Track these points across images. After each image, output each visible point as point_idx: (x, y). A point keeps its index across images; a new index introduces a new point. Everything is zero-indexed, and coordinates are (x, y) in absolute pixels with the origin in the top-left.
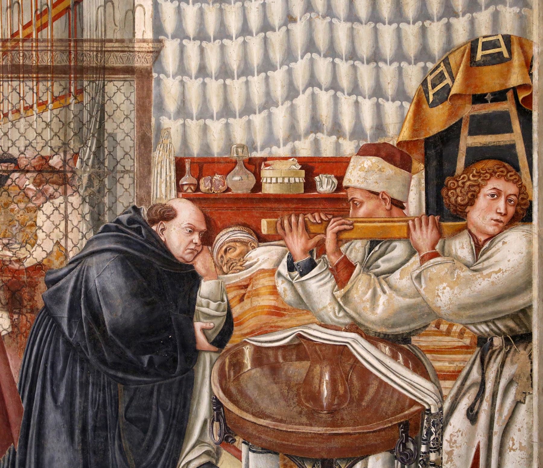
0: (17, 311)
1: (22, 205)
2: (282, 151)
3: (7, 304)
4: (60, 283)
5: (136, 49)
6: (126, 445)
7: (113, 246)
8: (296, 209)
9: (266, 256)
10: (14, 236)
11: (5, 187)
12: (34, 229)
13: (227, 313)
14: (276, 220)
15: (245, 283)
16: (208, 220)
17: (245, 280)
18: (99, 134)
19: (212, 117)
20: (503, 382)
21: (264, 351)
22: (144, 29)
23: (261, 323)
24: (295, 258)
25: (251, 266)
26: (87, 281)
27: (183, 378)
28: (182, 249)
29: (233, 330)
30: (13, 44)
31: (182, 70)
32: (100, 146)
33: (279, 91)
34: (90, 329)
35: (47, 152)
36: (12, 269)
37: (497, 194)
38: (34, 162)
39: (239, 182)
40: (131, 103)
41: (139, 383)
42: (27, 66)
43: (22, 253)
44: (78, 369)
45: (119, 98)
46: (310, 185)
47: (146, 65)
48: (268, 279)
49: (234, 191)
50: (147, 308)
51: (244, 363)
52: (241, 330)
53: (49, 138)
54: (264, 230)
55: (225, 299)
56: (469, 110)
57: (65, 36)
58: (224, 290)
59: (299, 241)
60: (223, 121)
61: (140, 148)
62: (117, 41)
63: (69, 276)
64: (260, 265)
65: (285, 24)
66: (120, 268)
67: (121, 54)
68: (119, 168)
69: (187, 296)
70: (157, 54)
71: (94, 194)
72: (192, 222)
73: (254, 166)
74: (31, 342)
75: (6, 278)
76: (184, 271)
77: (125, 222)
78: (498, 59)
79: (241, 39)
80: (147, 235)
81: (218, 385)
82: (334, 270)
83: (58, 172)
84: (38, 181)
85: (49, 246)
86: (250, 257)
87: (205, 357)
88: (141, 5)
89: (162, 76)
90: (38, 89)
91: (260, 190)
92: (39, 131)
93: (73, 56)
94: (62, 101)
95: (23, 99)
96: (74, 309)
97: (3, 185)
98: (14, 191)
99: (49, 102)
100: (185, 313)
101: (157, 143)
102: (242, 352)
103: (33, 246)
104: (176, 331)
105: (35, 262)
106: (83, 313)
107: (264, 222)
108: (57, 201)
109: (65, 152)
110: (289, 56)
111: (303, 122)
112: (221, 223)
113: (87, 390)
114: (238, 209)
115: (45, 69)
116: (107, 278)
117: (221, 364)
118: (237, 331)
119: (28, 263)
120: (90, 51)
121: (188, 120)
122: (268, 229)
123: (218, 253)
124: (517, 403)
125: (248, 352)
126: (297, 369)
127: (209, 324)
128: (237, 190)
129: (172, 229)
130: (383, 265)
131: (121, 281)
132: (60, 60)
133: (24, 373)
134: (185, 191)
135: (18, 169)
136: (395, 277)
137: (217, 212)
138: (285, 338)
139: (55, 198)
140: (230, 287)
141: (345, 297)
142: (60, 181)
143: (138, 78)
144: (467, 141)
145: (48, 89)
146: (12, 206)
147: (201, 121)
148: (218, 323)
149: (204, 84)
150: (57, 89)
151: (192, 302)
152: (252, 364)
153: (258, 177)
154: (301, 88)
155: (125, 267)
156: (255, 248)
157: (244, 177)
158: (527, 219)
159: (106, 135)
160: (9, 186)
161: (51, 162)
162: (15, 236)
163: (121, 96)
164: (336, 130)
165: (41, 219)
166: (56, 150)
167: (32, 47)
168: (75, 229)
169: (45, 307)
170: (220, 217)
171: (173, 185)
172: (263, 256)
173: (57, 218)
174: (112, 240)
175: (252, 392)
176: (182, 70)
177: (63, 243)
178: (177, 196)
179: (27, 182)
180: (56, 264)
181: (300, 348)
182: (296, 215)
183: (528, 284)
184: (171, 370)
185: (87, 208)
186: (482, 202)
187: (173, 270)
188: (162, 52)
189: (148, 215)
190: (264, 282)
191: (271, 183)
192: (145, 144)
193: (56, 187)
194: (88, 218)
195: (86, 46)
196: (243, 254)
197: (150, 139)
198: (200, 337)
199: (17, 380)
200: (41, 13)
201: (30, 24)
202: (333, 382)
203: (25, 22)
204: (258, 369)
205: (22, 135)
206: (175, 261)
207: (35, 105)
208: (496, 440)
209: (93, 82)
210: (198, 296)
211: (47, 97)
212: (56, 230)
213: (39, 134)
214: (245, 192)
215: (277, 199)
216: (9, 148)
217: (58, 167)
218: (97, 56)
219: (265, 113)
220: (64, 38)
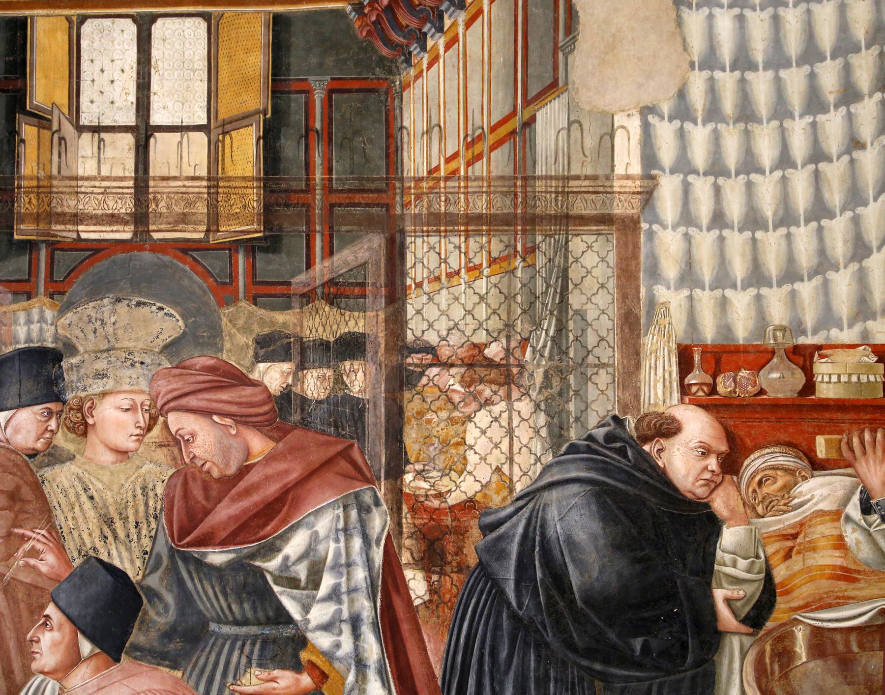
0: (437, 569)
1: (444, 414)
3: (422, 559)
4: (502, 529)
5: (616, 189)
7: (583, 474)
8: (871, 421)
9: (825, 491)
10: (433, 460)
11: (419, 388)
12: (461, 449)
13: (766, 576)
14: (839, 437)
15: (793, 532)
16: (730, 437)
17: (793, 526)
18: (560, 312)
19: (734, 286)
21: (826, 634)
23: (821, 591)
24: (873, 494)
25: (801, 505)
26: (543, 526)
27: (698, 673)
28: (691, 479)
29: (775, 601)
30: (431, 183)
32: (561, 328)
33: (839, 247)
34: (549, 597)
35: (481, 337)
36: (429, 507)
38: (462, 353)
39: (779, 381)
40: (608, 267)
41: (627, 679)
42: (452, 214)
43: (444, 484)
44: (532, 658)
45: (590, 260)
47: (630, 211)
48: (829, 525)
49: (771, 394)
50: (638, 567)
51: (795, 652)
52: (788, 602)
53: (484, 318)
54: (821, 452)
55: (762, 555)
57: (509, 171)
58: (760, 541)
59: (878, 468)
60: (752, 291)
61: (622, 330)
62: (587, 178)
63: (515, 518)
64: (816, 504)
65: (848, 151)
66: (594, 507)
67: (593, 196)
68: (591, 359)
69: (702, 550)
71: (552, 398)
72: (706, 439)
73: (803, 357)
74: (459, 616)
75: (420, 521)
76: (694, 511)
77: (601, 439)
79: (778, 174)
80: (636, 459)
81: (754, 685)
83: (498, 366)
84: (468, 379)
85: (484, 474)
86: (801, 493)
87: (731, 643)
88: (623, 127)
89: (655, 227)
90: (467, 247)
91: (813, 393)
92: (469, 307)
93: (520, 200)
94: (504, 264)
95: (445, 262)
97: (415, 386)
98: (431, 393)
99: (485, 265)
100: (698, 576)
101: (649, 324)
102: (791, 636)
103: (460, 474)
104: (685, 603)
105: (464, 497)
106: (539, 574)
107: (821, 441)
108: (496, 409)
109: (508, 338)
112: (751, 441)
113: (547, 688)
114: (778, 420)
115: (479, 219)
116: (573, 520)
117: (758, 653)
118: (781, 604)
119: (452, 500)
120: (546, 192)
121: (698, 290)
122: (827, 450)
123: (748, 486)
125: (800, 636)
127: (737, 592)
129: (675, 450)
131: (596, 526)
132: (501, 205)
133: (449, 662)
134: (694, 394)
135: (437, 362)
138: (860, 615)
139: (493, 404)
140: (768, 537)
142: (502, 379)
143: (618, 230)
145: (482, 247)
146: (428, 416)
147: (718, 293)
148: (753, 590)
149: (721, 239)
150: (496, 247)
152: (808, 654)
153: (809, 373)
154: (875, 244)
155: (602, 506)
156: (806, 478)
157: (787, 374)
159: (571, 313)
160: (424, 386)
161: (487, 351)
162: (434, 459)
163: (593, 258)
165: (472, 434)
166: (495, 335)
167: (459, 187)
168: (524, 450)
169: (480, 563)
170: (749, 433)
171: (675, 384)
172: (820, 491)
173: (496, 432)
174: (582, 465)
177: (506, 469)
178: (682, 401)
179: (452, 380)
180: (496, 500)
182: (871, 431)
184: (678, 661)
185: (542, 419)
187: (677, 510)
188: (655, 194)
189: (636, 428)
190: (823, 530)
191: (830, 382)
192: (631, 325)
193: (495, 387)
194: (544, 432)
195: (540, 185)
196: (787, 488)
197: (637, 318)
198: (723, 611)
199: (438, 672)
200: (473, 140)
201: (455, 155)
203: (449, 153)
204: (819, 662)
205: (443, 313)
206: (680, 497)
207: (463, 271)
209: (551, 236)
210: (718, 550)
211: (481, 259)
213: (469, 312)
214: (789, 395)
215: (840, 406)
216: (423, 332)
217: (497, 359)
218: (556, 200)
219: (817, 280)
220: (506, 174)
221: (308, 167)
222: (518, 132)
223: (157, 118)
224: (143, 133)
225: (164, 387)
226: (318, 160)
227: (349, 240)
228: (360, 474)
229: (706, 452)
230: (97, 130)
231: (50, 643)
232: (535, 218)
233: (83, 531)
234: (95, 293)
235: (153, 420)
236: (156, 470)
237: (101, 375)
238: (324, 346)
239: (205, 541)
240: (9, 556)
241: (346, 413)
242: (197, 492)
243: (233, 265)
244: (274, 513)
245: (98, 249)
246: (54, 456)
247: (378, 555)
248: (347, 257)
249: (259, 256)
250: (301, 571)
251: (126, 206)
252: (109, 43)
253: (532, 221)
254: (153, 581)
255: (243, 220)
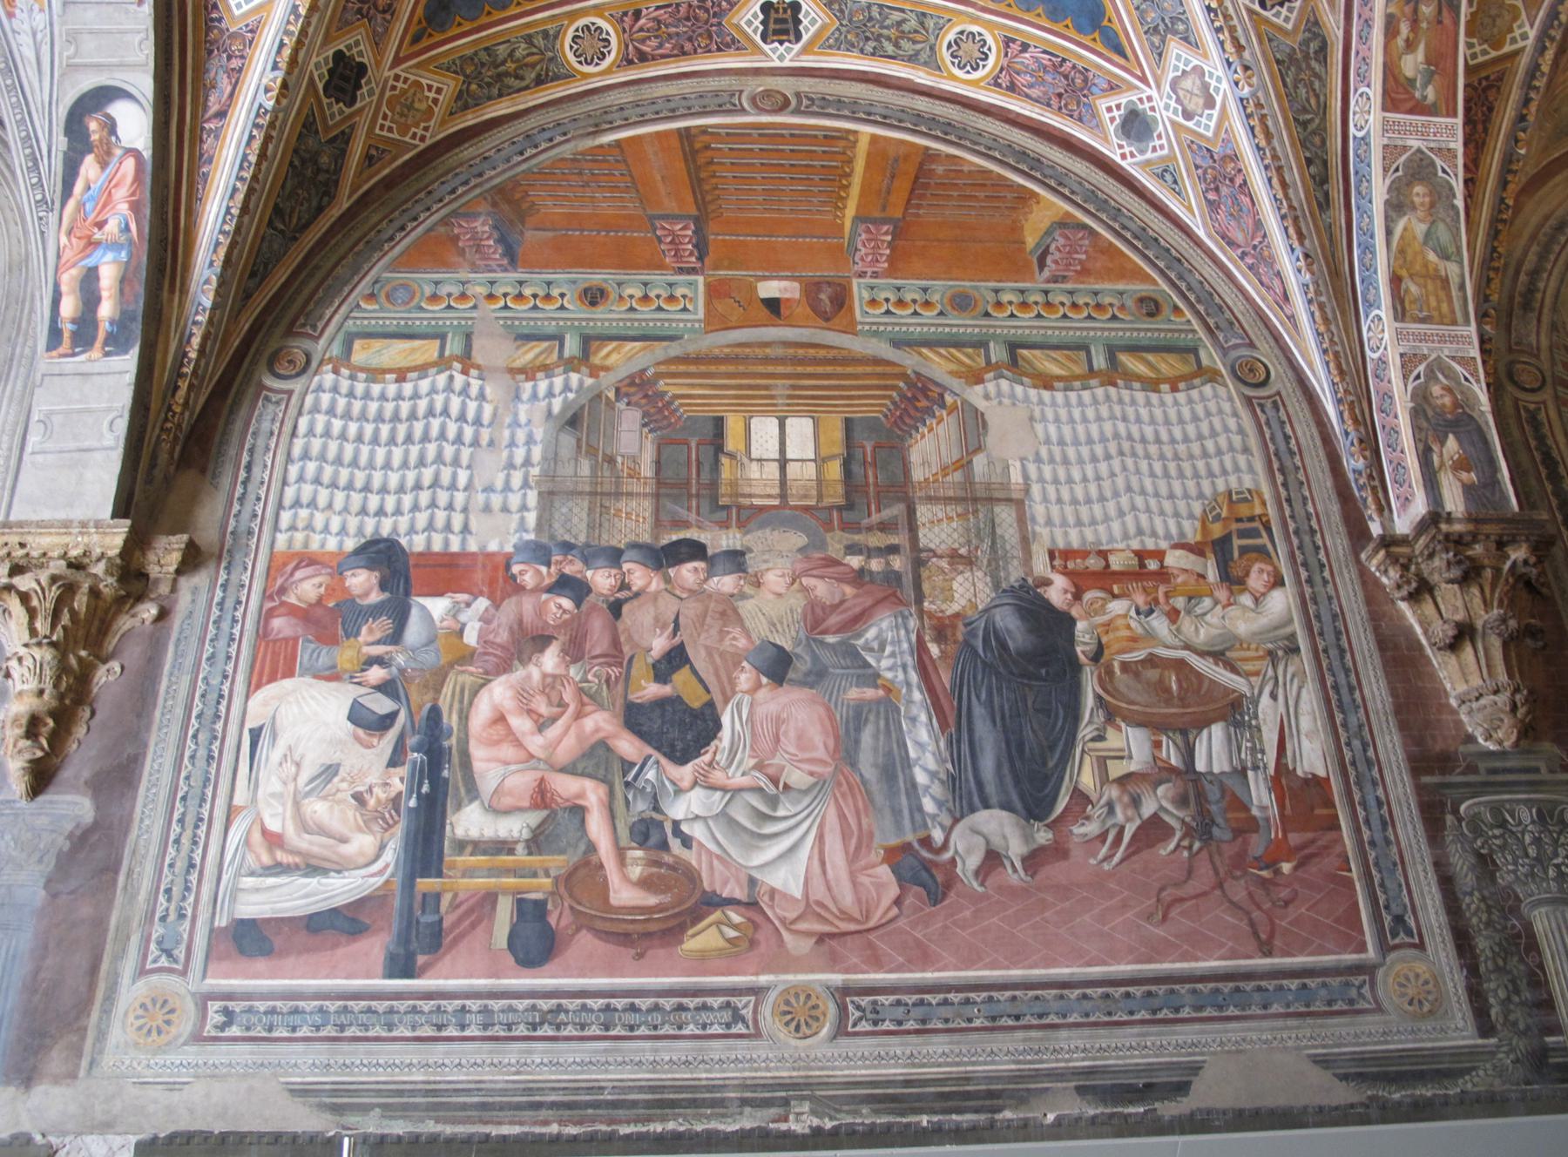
2: (1121, 546)
6: (1036, 726)
16: (1076, 586)
20: (1289, 677)
22: (1016, 477)
31: (1045, 499)
32: (994, 542)
35: (956, 546)
37: (1261, 571)
39: (1094, 563)
43: (944, 607)
45: (1004, 515)
46: (1142, 565)
56: (1234, 526)
70: (1027, 491)
78: (1246, 500)
82: (1168, 615)
85: (963, 602)
96: (986, 641)
98: (933, 569)
110: (1116, 494)
111: (1132, 530)
115: (950, 498)
116: (1008, 621)
118: (1106, 652)
119: (948, 613)
124: (1300, 688)
125: (1116, 665)
126: (1152, 674)
127: (1087, 648)
128: (1092, 568)
130: (1198, 610)
131: (1019, 623)
132: (960, 493)
135: (936, 555)
136: (1208, 617)
137: (1080, 583)
141: (1178, 630)
144: (1237, 542)
145: (951, 510)
150: (960, 510)
151: (1073, 634)
158: (1282, 584)
163: (1005, 516)
164: (1154, 534)
165: (955, 585)
172: (1117, 607)
173: (967, 585)
175: (1123, 689)
176: (1045, 499)
179: (944, 564)
180: (970, 613)
181: (1152, 661)
183: (1291, 621)
186: (1253, 575)
192: (1026, 542)
196: (1103, 606)
198: (1082, 657)
202: (1179, 681)
208: (1292, 710)
212: (966, 593)
221: (866, 477)
222: (964, 465)
223: (789, 456)
224: (783, 462)
225: (799, 566)
226: (870, 474)
227: (888, 506)
228: (901, 602)
229: (1066, 592)
230: (759, 460)
231: (745, 678)
232: (976, 499)
233: (761, 630)
234: (762, 526)
235: (794, 581)
236: (797, 602)
237: (766, 561)
238: (879, 549)
239: (825, 632)
240: (721, 640)
241: (893, 578)
242: (819, 611)
243: (831, 515)
244: (858, 620)
245: (762, 509)
246: (743, 596)
247: (914, 637)
248: (886, 514)
249: (845, 514)
250: (875, 645)
251: (776, 491)
252: (764, 431)
253: (975, 500)
254: (798, 650)
255: (836, 495)
